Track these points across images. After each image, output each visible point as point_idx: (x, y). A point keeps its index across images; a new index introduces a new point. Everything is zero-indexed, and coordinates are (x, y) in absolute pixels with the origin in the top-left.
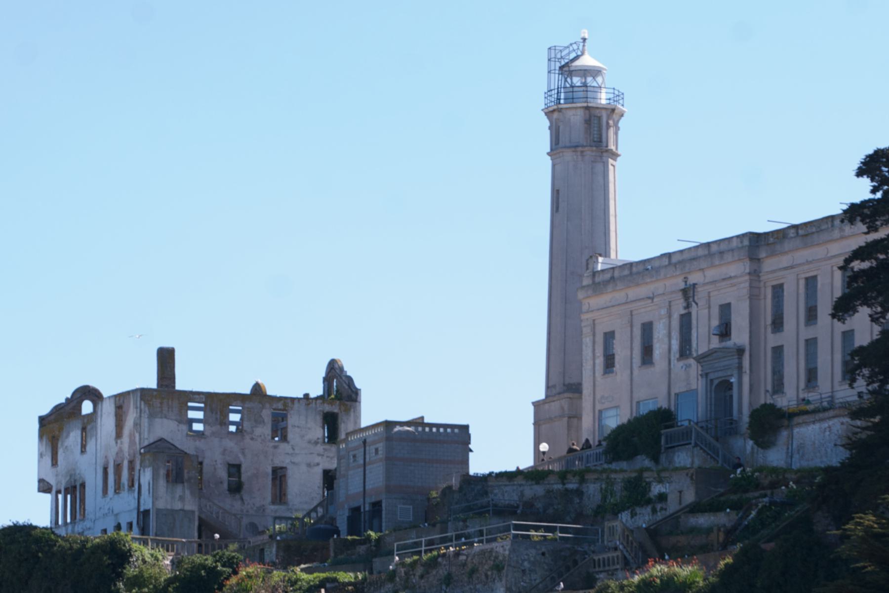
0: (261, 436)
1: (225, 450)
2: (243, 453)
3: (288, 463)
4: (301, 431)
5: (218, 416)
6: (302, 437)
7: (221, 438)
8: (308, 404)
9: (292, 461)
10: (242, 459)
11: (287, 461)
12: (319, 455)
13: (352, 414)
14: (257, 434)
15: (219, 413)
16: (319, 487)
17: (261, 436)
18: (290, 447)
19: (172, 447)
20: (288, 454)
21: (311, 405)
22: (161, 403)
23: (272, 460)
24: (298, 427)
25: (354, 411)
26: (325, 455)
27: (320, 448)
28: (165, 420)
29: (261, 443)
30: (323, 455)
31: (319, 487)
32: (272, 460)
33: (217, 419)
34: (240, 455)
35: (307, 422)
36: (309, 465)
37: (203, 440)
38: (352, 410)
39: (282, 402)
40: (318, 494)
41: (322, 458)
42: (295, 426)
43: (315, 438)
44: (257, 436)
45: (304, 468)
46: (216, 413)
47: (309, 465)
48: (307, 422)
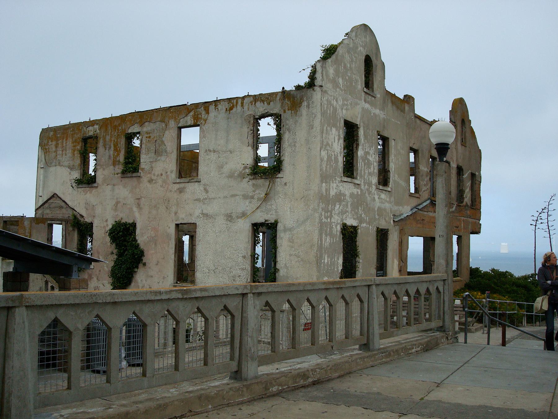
0: (162, 175)
1: (117, 203)
2: (139, 205)
3: (198, 217)
4: (219, 157)
5: (112, 153)
6: (221, 167)
7: (114, 185)
8: (231, 109)
9: (205, 211)
10: (137, 215)
11: (198, 212)
12: (245, 197)
13: (304, 110)
14: (156, 174)
15: (112, 148)
16: (244, 257)
17: (162, 175)
18: (202, 189)
19: (63, 204)
20: (198, 200)
21: (234, 109)
22: (56, 147)
23: (176, 213)
24: (214, 151)
25: (308, 106)
26: (256, 197)
27: (247, 185)
28: (58, 168)
29: (161, 186)
30: (252, 197)
31: (244, 257)
32: (176, 213)
33: (110, 156)
34: (135, 209)
35: (227, 141)
36: (229, 217)
37: (94, 190)
38: (305, 104)
39: (192, 113)
40: (243, 269)
41: (250, 202)
42: (210, 151)
43: (240, 168)
44: (158, 175)
45: (221, 221)
46: (110, 148)
47: (229, 217)
48: (227, 141)
